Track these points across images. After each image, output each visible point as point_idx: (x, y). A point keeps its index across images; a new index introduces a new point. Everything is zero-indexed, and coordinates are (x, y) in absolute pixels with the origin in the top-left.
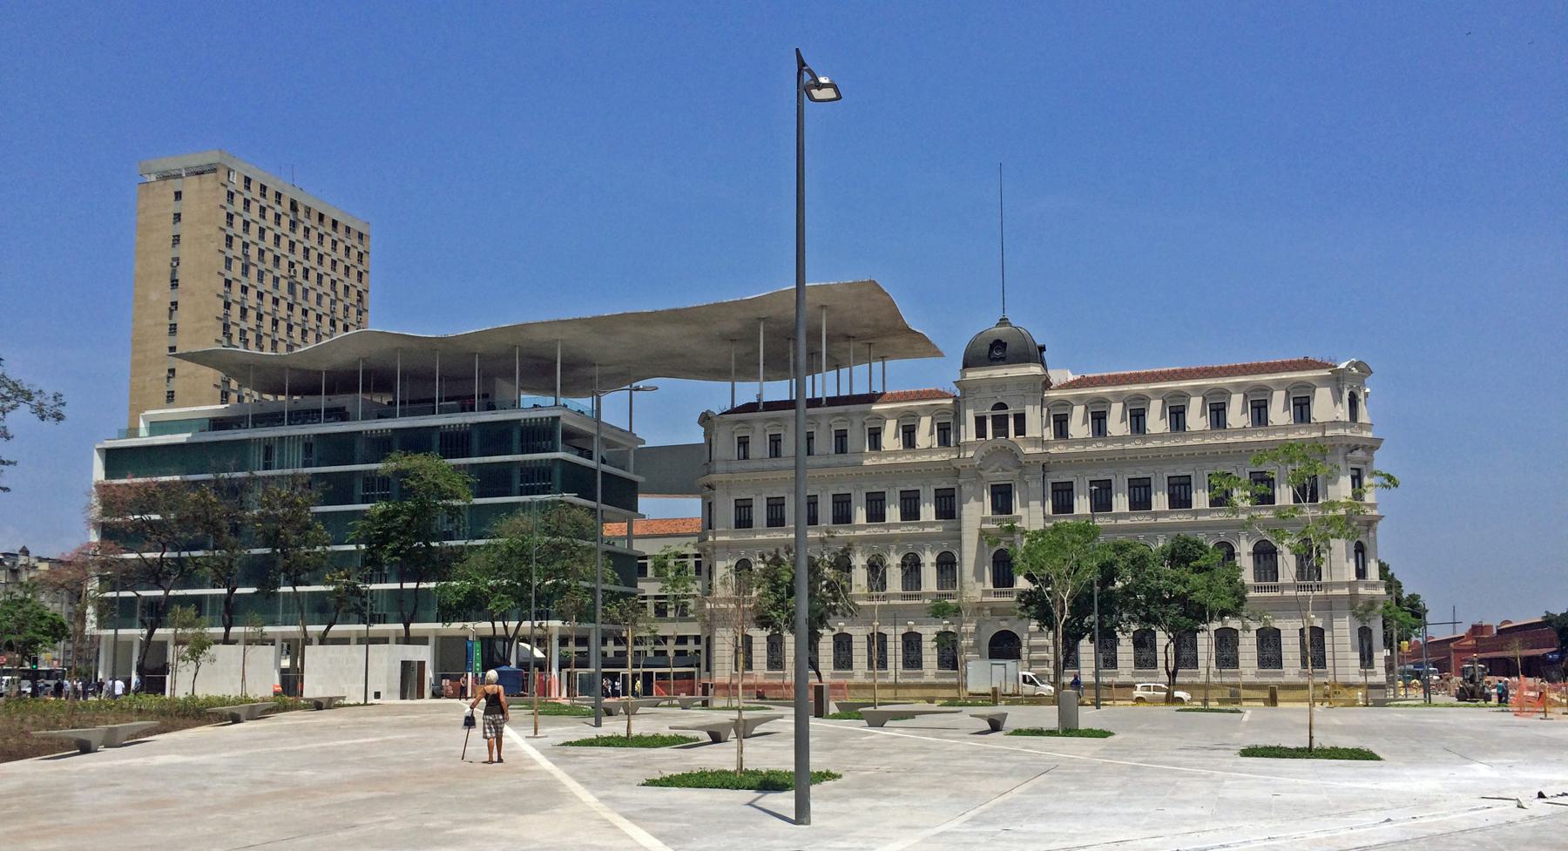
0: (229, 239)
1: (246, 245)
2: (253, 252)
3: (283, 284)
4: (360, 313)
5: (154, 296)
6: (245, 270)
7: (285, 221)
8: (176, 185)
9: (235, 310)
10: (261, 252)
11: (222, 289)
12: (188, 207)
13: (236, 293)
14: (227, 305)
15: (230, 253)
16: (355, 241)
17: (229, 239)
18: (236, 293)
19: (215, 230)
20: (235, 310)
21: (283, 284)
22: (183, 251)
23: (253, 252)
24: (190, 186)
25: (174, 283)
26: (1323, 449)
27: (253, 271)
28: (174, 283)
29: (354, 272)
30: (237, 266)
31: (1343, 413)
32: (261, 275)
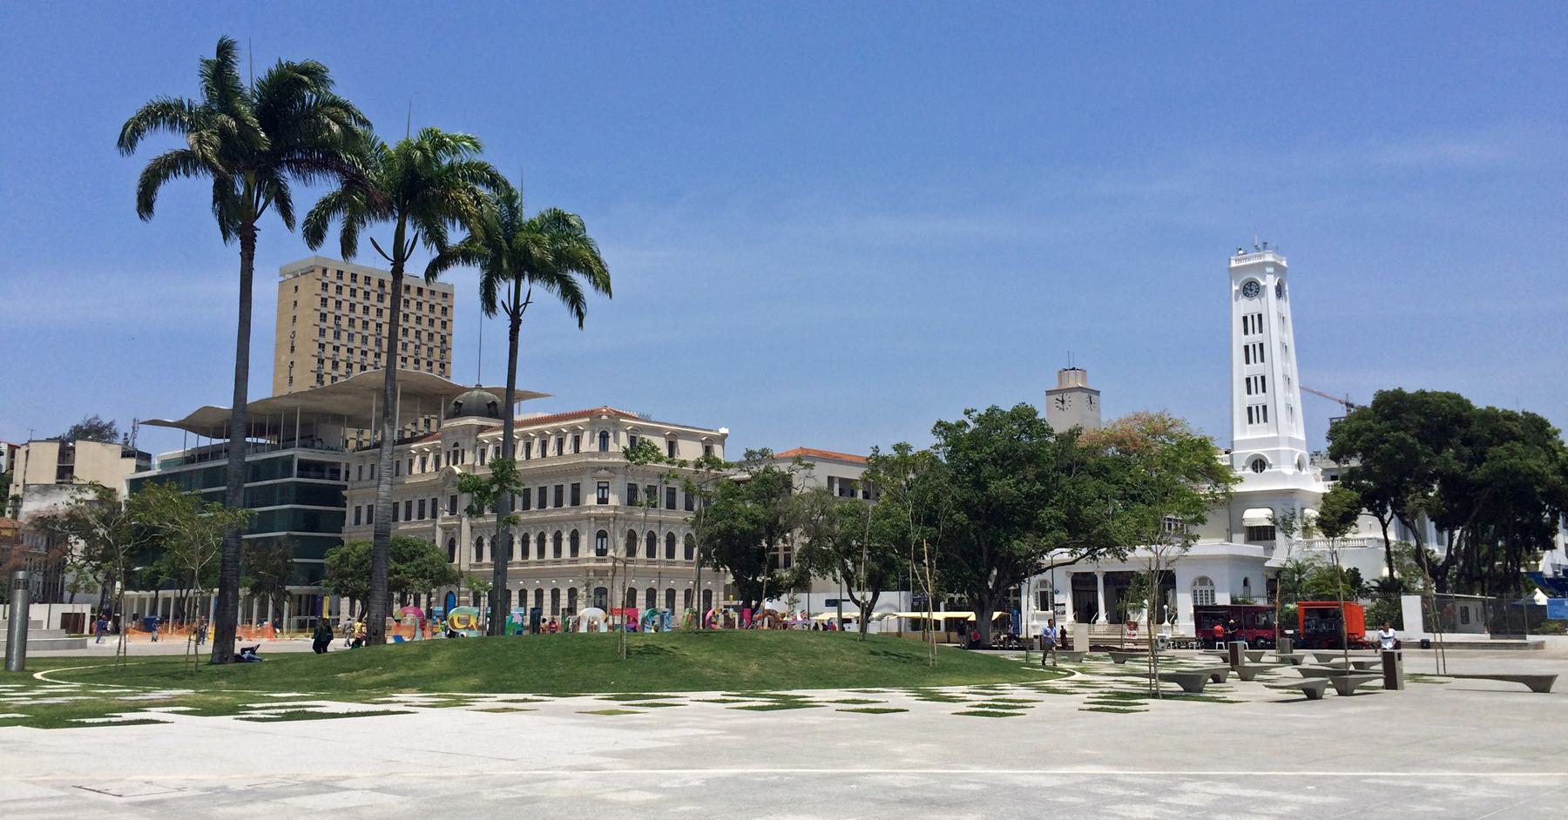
0: (323, 317)
1: (338, 318)
2: (344, 322)
3: (371, 340)
4: (443, 351)
5: (283, 358)
6: (337, 335)
7: (374, 297)
8: (296, 282)
9: (328, 364)
10: (352, 321)
11: (316, 350)
12: (302, 297)
13: (329, 351)
14: (321, 361)
15: (323, 325)
16: (439, 300)
17: (323, 317)
18: (329, 351)
19: (310, 311)
20: (328, 364)
21: (371, 340)
22: (298, 327)
23: (344, 322)
24: (302, 282)
25: (293, 349)
26: (581, 470)
27: (344, 336)
28: (293, 349)
29: (438, 323)
30: (330, 334)
31: (595, 447)
32: (351, 337)
